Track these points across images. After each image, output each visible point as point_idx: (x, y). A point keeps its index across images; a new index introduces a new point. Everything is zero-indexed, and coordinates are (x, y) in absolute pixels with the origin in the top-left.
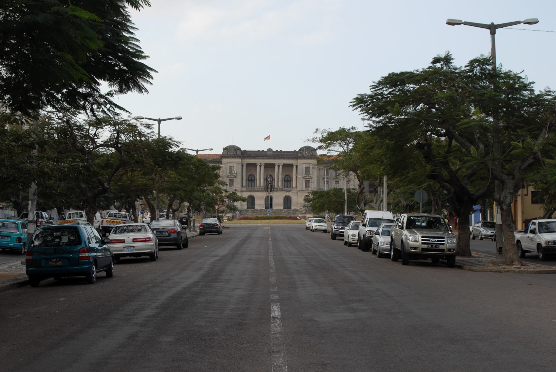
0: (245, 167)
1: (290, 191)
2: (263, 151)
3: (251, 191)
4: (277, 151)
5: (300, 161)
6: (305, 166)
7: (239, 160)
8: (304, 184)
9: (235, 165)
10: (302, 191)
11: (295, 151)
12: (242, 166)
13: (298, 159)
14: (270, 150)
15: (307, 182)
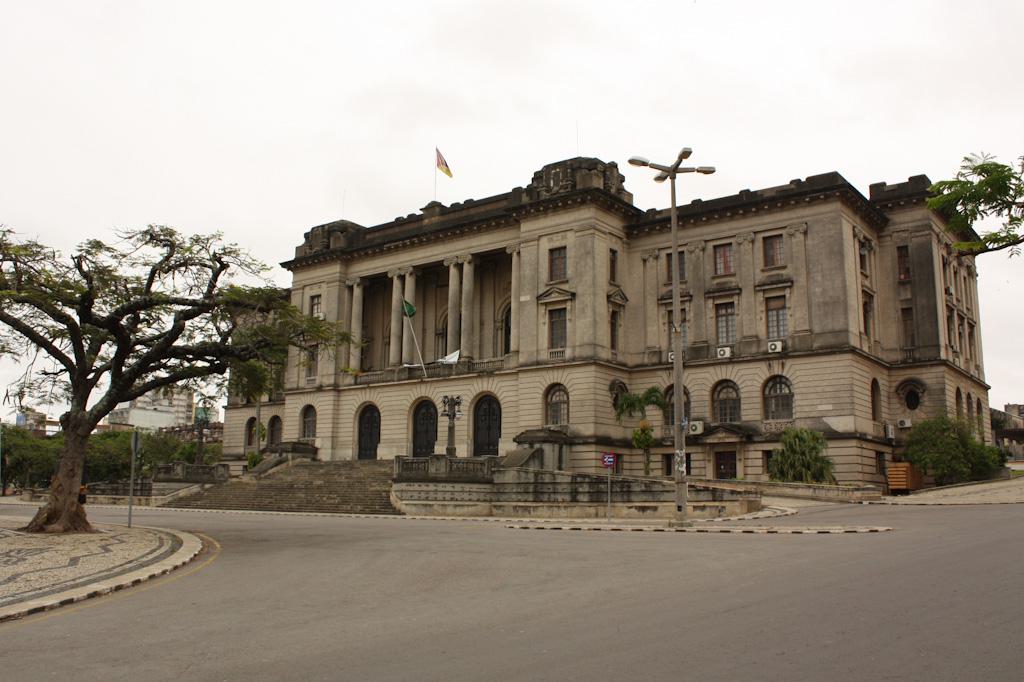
0: (357, 292)
1: (490, 374)
2: (411, 216)
3: (368, 386)
4: (455, 206)
5: (528, 227)
6: (545, 245)
7: (334, 270)
8: (545, 330)
9: (323, 290)
10: (537, 366)
11: (517, 191)
12: (351, 288)
13: (517, 223)
14: (434, 207)
15: (557, 317)
